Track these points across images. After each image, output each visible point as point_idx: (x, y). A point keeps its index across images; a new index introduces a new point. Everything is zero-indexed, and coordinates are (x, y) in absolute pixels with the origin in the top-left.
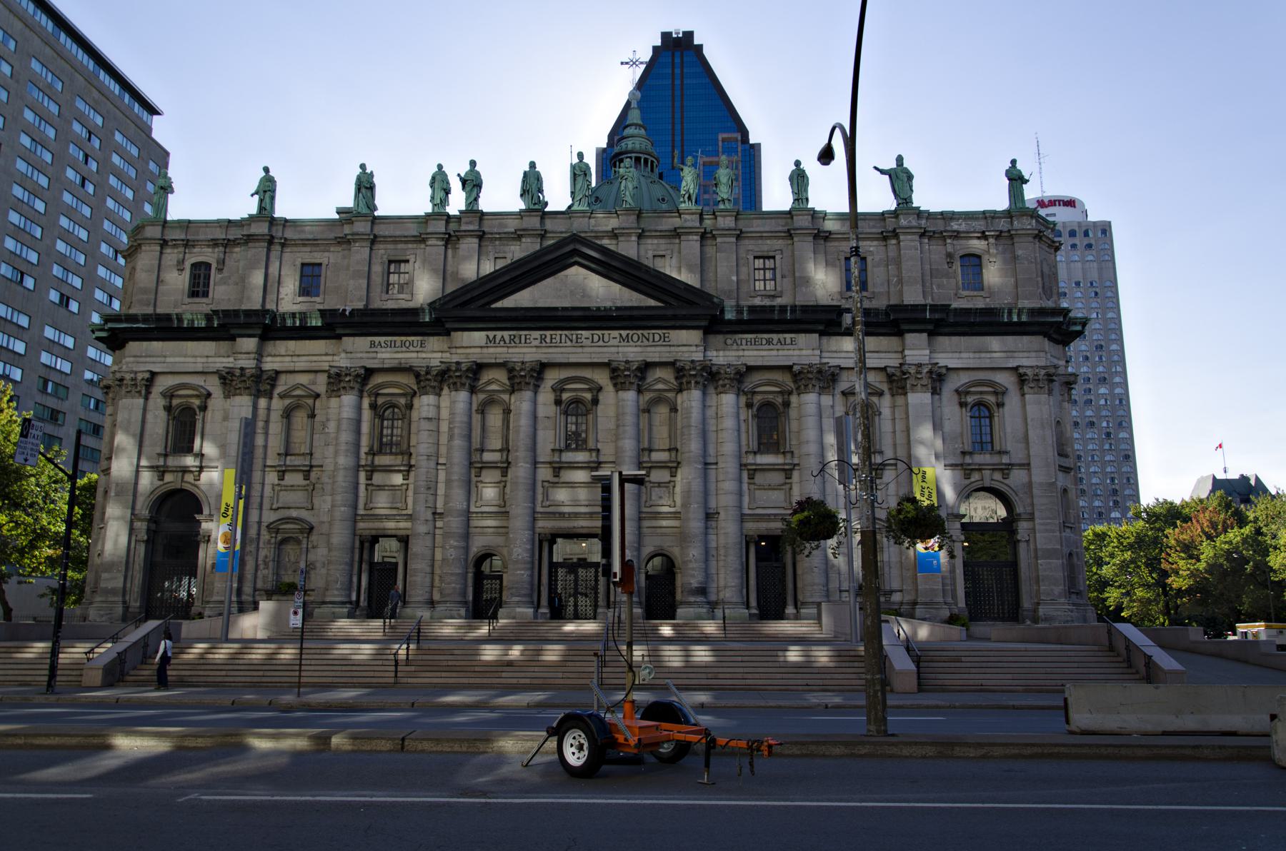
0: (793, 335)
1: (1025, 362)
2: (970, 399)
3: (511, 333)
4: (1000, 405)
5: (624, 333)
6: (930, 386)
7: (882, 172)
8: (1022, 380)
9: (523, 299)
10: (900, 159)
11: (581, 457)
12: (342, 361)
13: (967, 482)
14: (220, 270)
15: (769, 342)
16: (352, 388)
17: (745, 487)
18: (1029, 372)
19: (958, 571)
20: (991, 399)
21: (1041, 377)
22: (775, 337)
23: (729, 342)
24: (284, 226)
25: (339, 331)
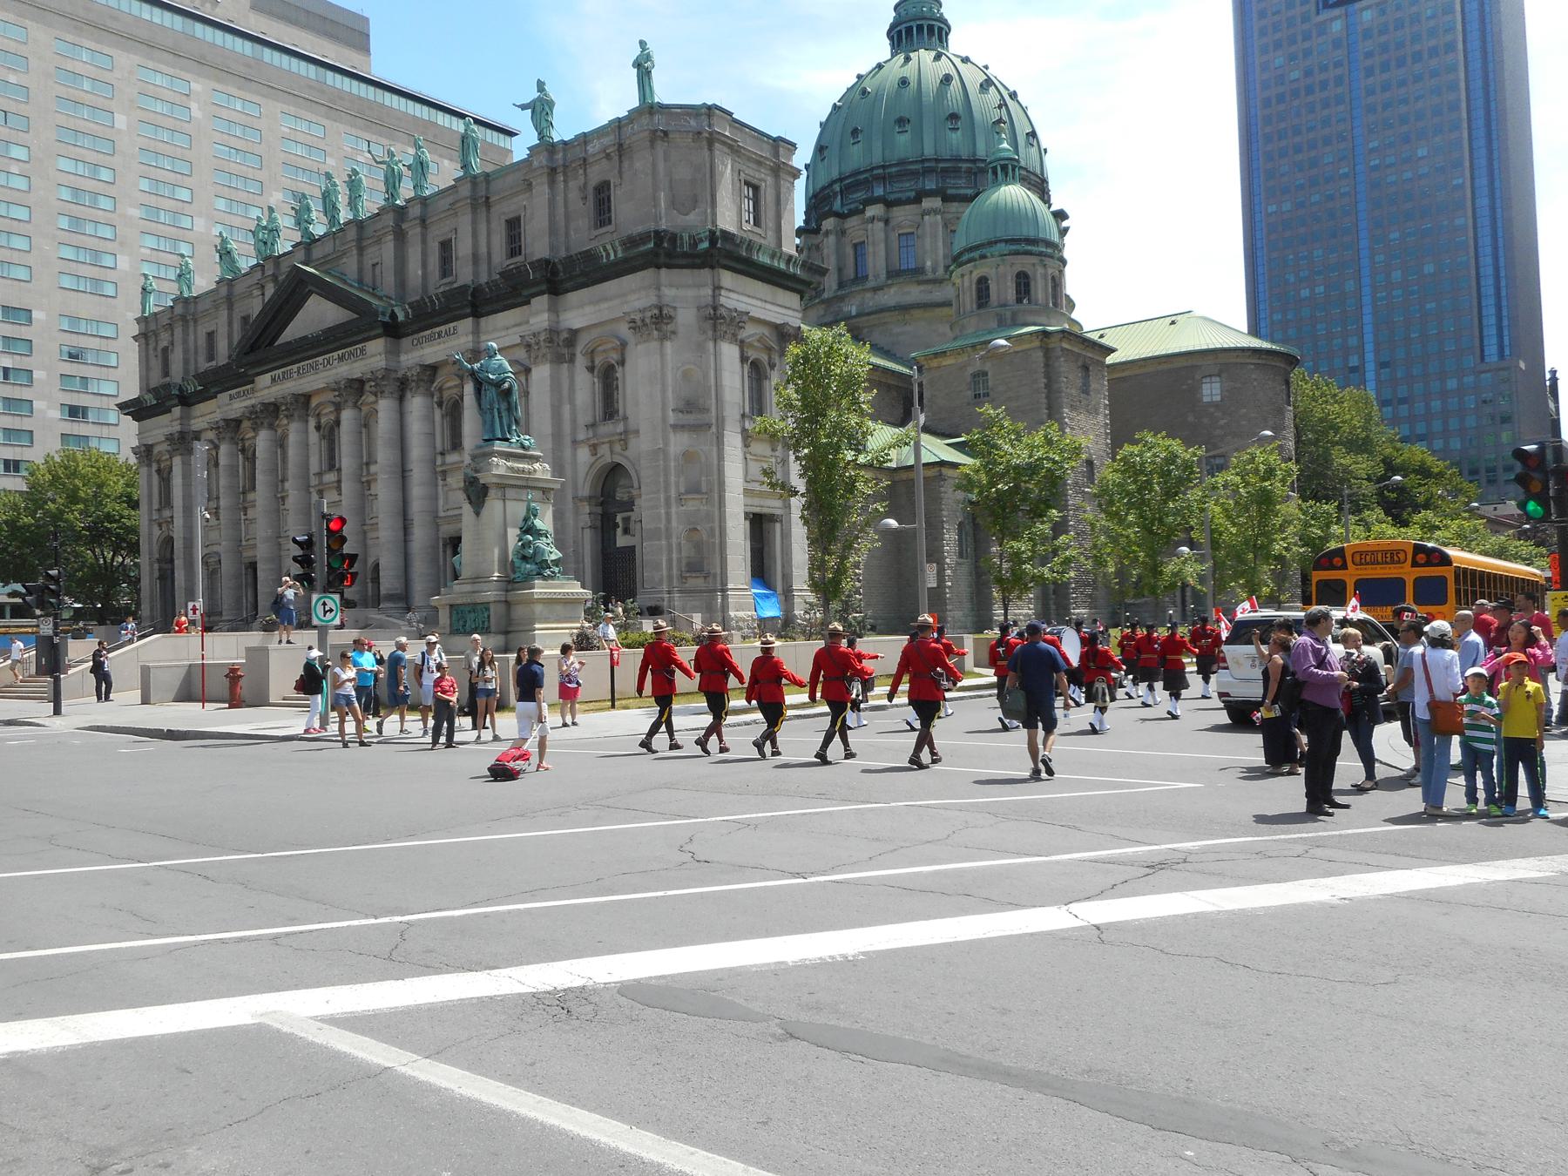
0: (455, 324)
1: (639, 304)
2: (598, 361)
3: (283, 370)
4: (622, 363)
5: (340, 352)
6: (549, 356)
7: (523, 107)
8: (635, 326)
9: (293, 331)
10: (541, 86)
11: (330, 477)
12: (217, 416)
13: (594, 458)
14: (172, 350)
15: (439, 336)
16: (224, 438)
17: (440, 488)
18: (638, 317)
19: (586, 560)
20: (614, 357)
21: (648, 321)
22: (443, 328)
23: (415, 342)
24: (196, 303)
25: (213, 390)
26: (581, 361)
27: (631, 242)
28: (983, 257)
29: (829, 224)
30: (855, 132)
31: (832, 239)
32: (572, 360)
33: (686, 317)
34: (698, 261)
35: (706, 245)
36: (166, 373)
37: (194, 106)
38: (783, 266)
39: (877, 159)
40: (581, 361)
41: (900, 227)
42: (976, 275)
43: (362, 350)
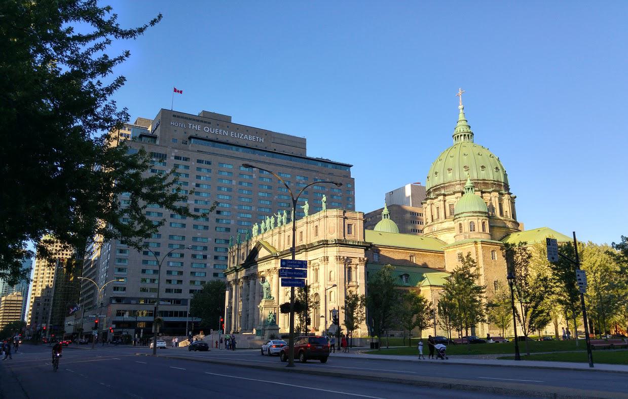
20: (317, 267)
26: (312, 268)
27: (318, 242)
28: (459, 218)
29: (428, 201)
30: (436, 173)
31: (430, 206)
32: (310, 268)
33: (332, 259)
34: (334, 245)
35: (334, 242)
36: (234, 263)
37: (254, 175)
38: (356, 244)
39: (442, 182)
40: (312, 268)
41: (449, 202)
42: (459, 222)
43: (271, 262)
